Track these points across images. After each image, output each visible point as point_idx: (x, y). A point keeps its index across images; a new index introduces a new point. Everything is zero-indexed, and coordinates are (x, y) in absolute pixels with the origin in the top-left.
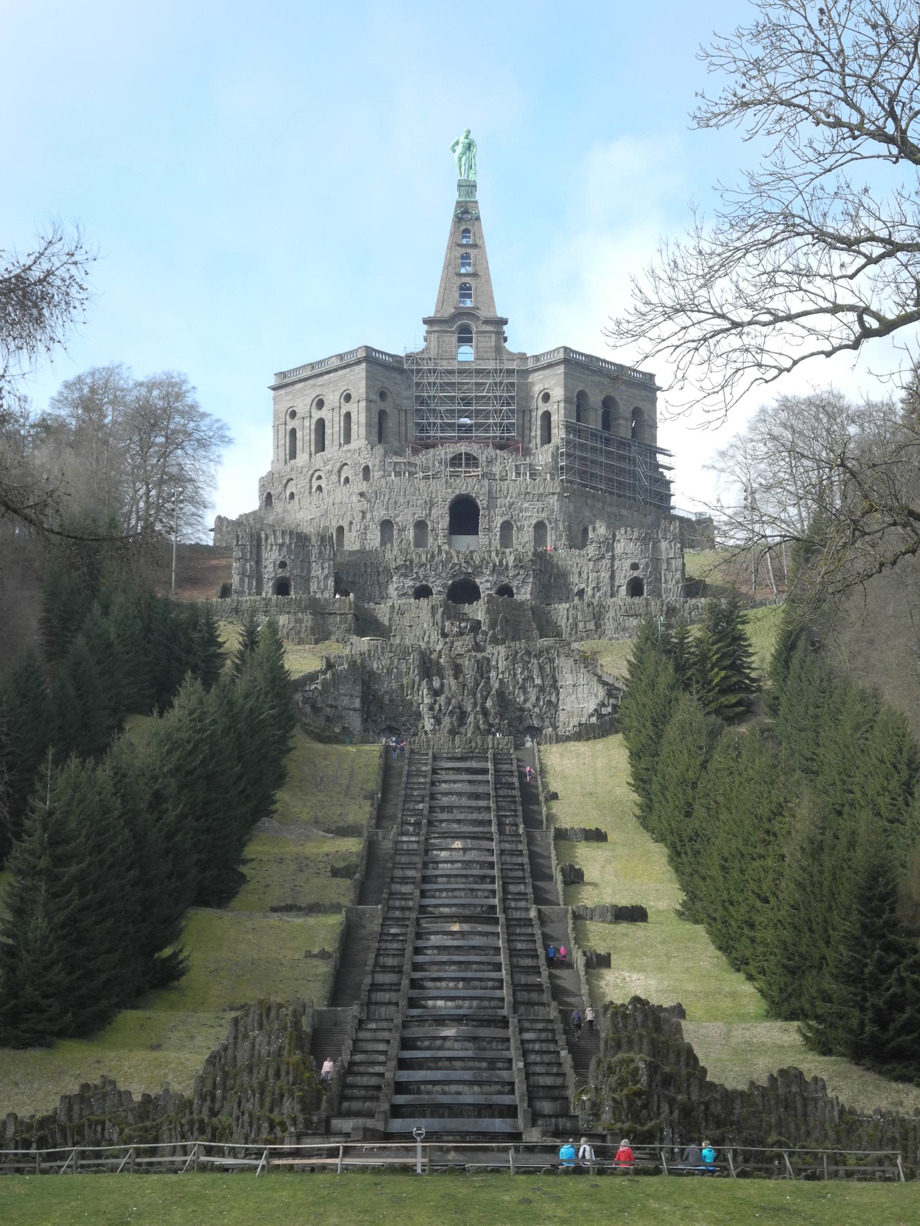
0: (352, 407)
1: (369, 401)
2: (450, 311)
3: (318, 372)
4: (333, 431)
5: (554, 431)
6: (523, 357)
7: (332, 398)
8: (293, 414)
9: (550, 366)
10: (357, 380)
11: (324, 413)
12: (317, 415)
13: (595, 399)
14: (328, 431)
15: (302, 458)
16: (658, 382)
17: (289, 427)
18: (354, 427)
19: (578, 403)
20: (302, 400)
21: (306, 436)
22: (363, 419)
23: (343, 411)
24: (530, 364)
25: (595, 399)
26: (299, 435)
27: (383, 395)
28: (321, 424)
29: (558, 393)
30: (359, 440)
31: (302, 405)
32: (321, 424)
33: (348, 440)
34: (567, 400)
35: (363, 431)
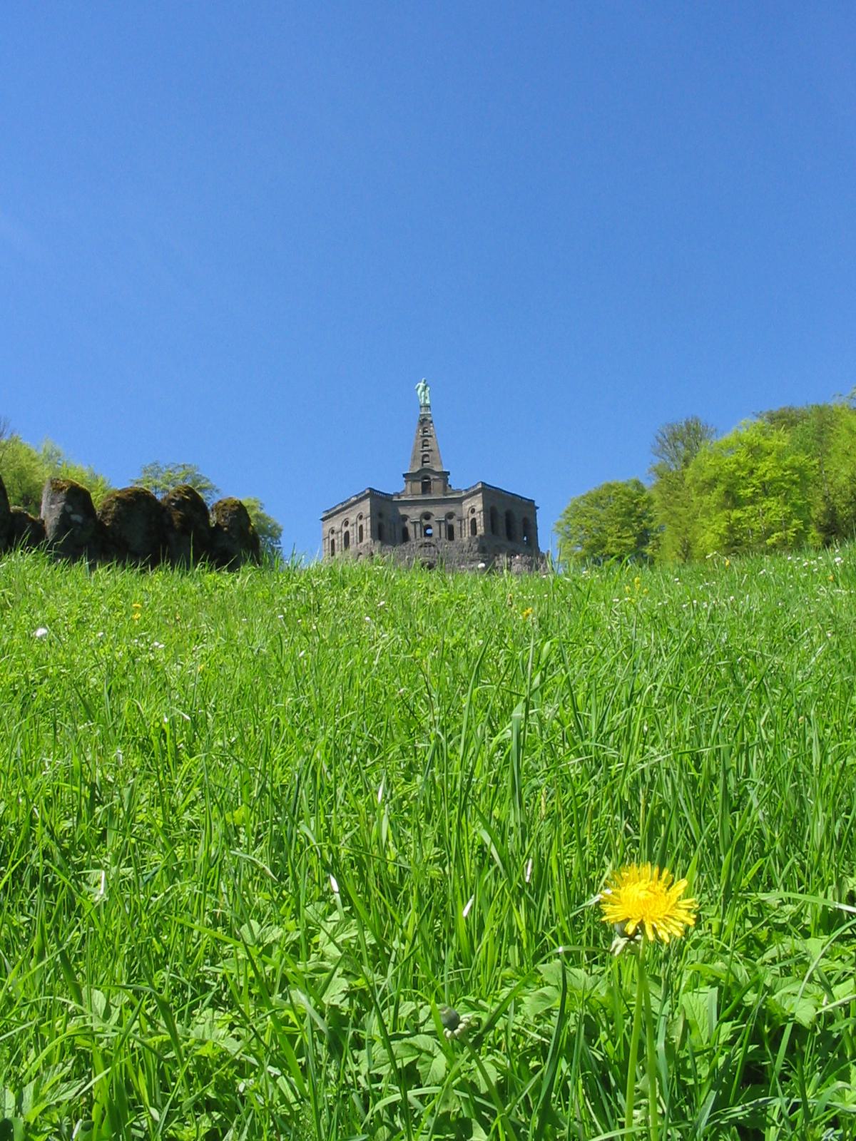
0: (363, 522)
1: (371, 516)
2: (417, 469)
3: (347, 506)
4: (354, 536)
5: (479, 528)
6: (459, 491)
7: (353, 519)
8: (333, 532)
9: (475, 493)
10: (365, 507)
11: (349, 528)
12: (345, 530)
13: (501, 511)
14: (351, 537)
15: (338, 554)
16: (536, 504)
17: (331, 539)
18: (364, 532)
19: (491, 514)
20: (336, 523)
21: (339, 541)
22: (369, 527)
23: (359, 525)
24: (464, 494)
25: (501, 511)
26: (336, 542)
27: (380, 515)
28: (347, 534)
29: (479, 507)
30: (367, 539)
31: (337, 526)
32: (347, 534)
33: (361, 540)
34: (484, 510)
35: (369, 533)
